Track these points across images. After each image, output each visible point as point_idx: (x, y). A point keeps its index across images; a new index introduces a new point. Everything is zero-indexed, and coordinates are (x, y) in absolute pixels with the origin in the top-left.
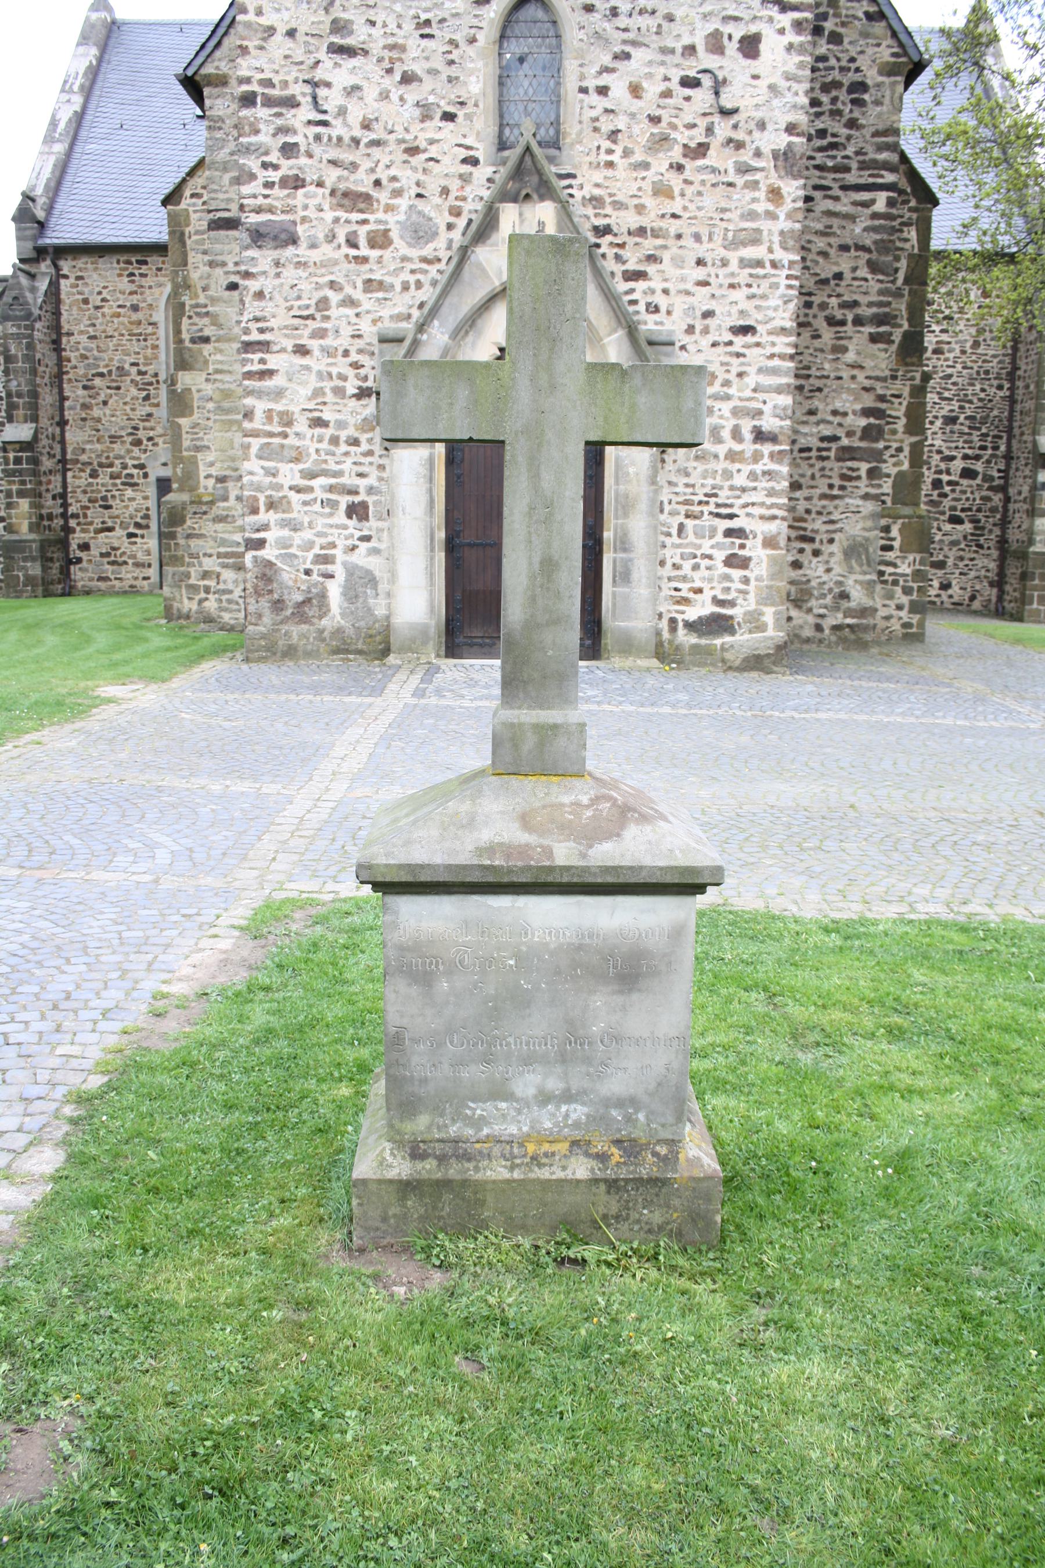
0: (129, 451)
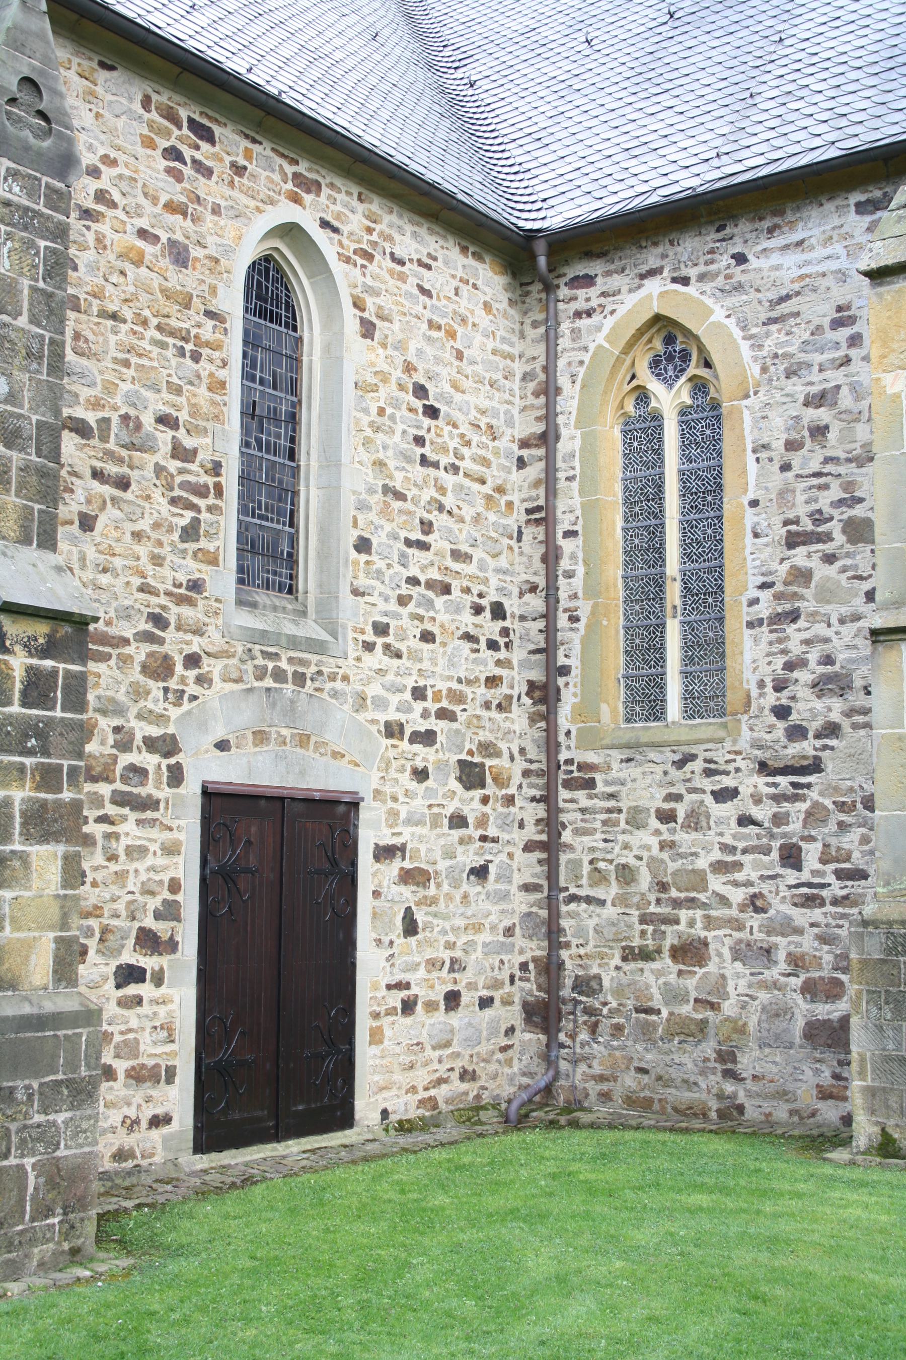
0: (138, 693)
